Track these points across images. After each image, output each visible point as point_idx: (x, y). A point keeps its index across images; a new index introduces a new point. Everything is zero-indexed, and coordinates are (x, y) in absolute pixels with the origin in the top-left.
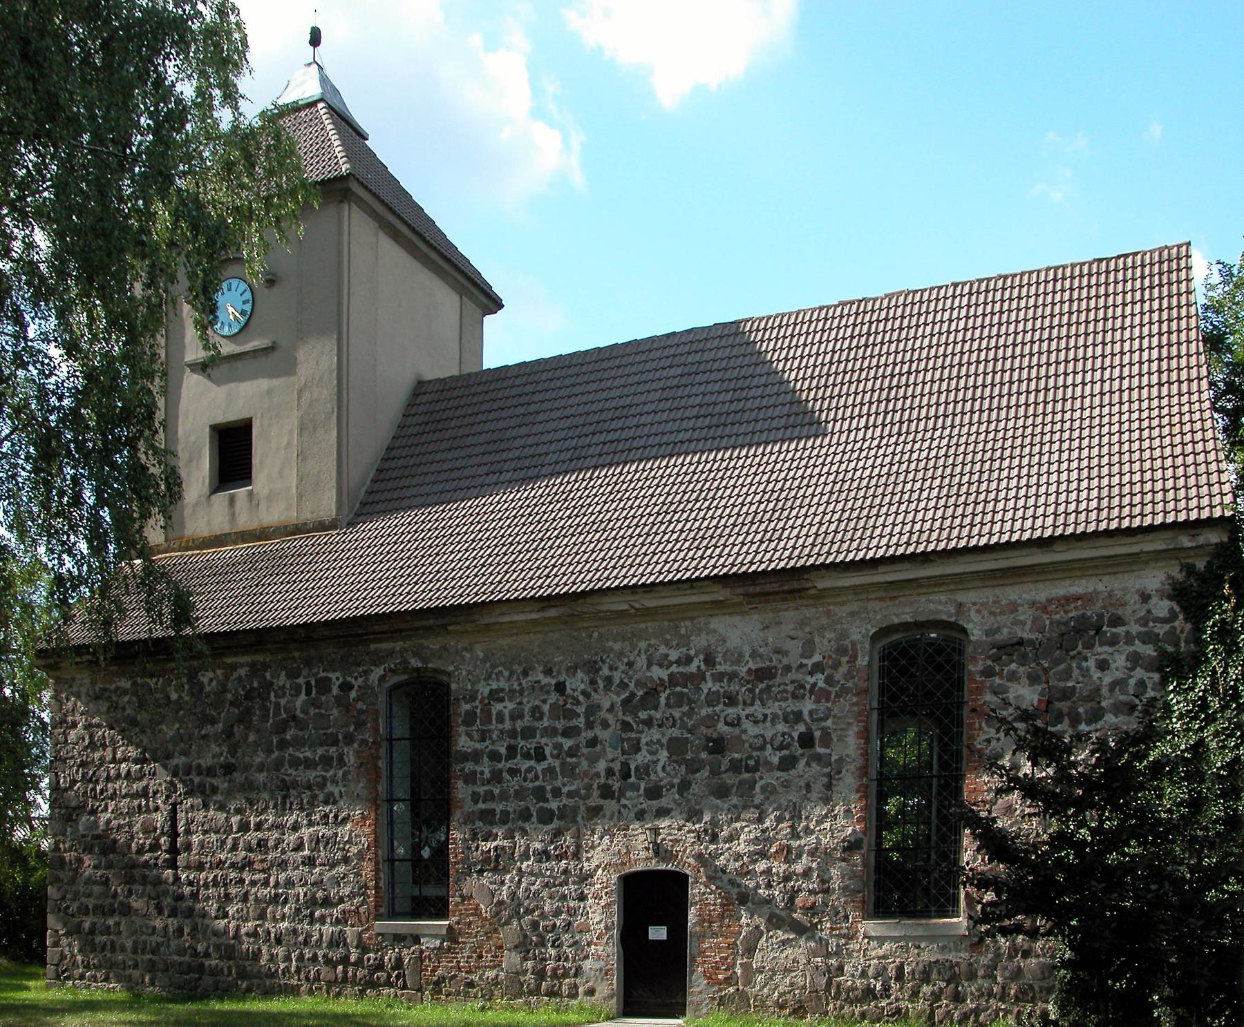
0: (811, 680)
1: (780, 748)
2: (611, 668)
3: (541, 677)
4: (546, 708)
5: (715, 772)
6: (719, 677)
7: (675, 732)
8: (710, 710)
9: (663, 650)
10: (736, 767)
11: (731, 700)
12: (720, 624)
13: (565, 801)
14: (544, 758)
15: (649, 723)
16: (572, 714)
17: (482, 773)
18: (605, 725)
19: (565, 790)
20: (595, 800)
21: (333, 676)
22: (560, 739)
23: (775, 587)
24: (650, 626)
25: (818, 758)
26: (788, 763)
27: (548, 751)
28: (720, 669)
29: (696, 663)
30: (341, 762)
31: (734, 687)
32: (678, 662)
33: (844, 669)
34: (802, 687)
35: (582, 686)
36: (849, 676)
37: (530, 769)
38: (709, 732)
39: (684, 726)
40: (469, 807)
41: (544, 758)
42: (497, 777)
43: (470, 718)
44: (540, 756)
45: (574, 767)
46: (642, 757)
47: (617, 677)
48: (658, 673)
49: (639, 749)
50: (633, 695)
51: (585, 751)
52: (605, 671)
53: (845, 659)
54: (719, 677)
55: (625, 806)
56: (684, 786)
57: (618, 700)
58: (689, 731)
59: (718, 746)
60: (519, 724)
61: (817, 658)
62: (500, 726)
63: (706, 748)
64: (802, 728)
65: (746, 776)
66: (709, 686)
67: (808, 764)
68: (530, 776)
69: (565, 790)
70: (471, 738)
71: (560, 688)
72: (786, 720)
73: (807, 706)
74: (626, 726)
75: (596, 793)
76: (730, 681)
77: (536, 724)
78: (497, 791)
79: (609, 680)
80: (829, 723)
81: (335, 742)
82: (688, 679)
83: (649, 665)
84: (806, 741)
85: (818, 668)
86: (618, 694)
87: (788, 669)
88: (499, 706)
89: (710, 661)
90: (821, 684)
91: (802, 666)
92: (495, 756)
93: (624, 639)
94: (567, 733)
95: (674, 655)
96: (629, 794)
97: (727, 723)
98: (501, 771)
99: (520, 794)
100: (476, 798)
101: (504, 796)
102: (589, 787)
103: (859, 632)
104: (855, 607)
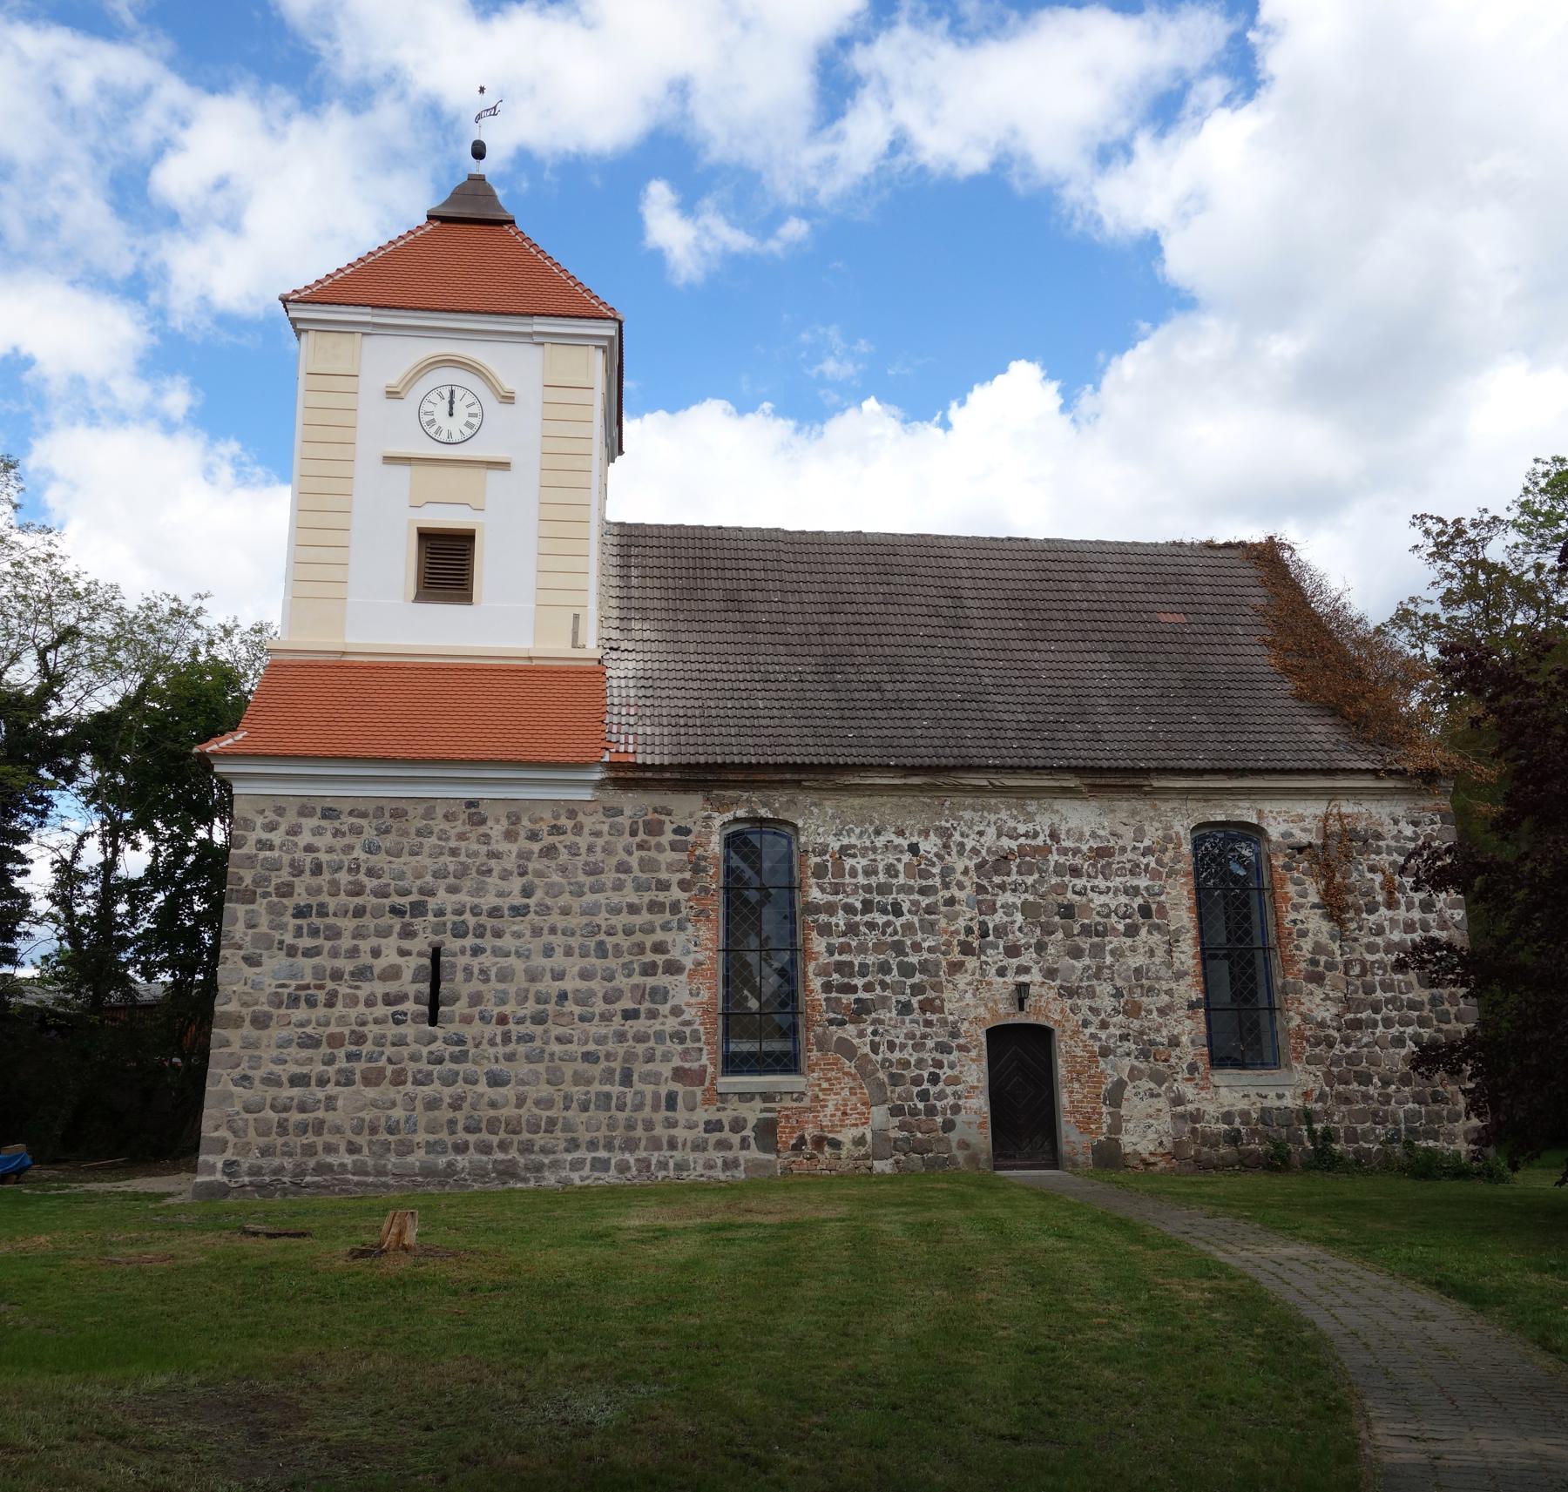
0: (1145, 861)
2: (962, 835)
3: (893, 837)
4: (901, 867)
5: (1068, 934)
6: (1064, 851)
7: (1031, 898)
8: (1059, 879)
9: (1011, 823)
10: (1086, 931)
11: (1075, 872)
13: (926, 955)
14: (902, 914)
15: (1002, 887)
16: (925, 874)
17: (837, 925)
18: (961, 887)
19: (925, 945)
20: (956, 956)
22: (916, 897)
23: (1118, 781)
25: (1158, 928)
26: (1132, 931)
27: (905, 907)
28: (1065, 844)
31: (1078, 861)
32: (1026, 835)
34: (1138, 866)
35: (935, 849)
36: (1176, 860)
37: (888, 924)
38: (1060, 899)
39: (1035, 893)
40: (824, 959)
41: (902, 914)
42: (852, 929)
43: (820, 871)
45: (932, 924)
46: (999, 917)
48: (1006, 843)
49: (995, 911)
50: (984, 862)
51: (943, 909)
52: (957, 837)
53: (1171, 846)
54: (1064, 851)
55: (987, 963)
56: (1041, 947)
57: (971, 864)
58: (1042, 897)
59: (1068, 911)
60: (873, 881)
61: (1147, 843)
62: (854, 881)
63: (1058, 914)
64: (1140, 900)
65: (1096, 939)
66: (1054, 857)
67: (1149, 932)
68: (889, 930)
69: (925, 945)
70: (823, 890)
71: (914, 849)
72: (1126, 892)
73: (1143, 882)
75: (957, 949)
76: (1074, 855)
77: (894, 881)
78: (854, 944)
79: (962, 845)
80: (1163, 898)
82: (1036, 850)
83: (999, 836)
84: (1145, 911)
85: (1147, 852)
86: (971, 859)
87: (1123, 850)
89: (1054, 835)
90: (1153, 865)
91: (1135, 848)
92: (849, 909)
93: (974, 810)
94: (923, 891)
95: (1022, 829)
96: (989, 952)
97: (1075, 892)
98: (857, 924)
99: (879, 947)
100: (830, 950)
101: (862, 949)
102: (948, 944)
103: (1182, 827)
104: (1175, 804)
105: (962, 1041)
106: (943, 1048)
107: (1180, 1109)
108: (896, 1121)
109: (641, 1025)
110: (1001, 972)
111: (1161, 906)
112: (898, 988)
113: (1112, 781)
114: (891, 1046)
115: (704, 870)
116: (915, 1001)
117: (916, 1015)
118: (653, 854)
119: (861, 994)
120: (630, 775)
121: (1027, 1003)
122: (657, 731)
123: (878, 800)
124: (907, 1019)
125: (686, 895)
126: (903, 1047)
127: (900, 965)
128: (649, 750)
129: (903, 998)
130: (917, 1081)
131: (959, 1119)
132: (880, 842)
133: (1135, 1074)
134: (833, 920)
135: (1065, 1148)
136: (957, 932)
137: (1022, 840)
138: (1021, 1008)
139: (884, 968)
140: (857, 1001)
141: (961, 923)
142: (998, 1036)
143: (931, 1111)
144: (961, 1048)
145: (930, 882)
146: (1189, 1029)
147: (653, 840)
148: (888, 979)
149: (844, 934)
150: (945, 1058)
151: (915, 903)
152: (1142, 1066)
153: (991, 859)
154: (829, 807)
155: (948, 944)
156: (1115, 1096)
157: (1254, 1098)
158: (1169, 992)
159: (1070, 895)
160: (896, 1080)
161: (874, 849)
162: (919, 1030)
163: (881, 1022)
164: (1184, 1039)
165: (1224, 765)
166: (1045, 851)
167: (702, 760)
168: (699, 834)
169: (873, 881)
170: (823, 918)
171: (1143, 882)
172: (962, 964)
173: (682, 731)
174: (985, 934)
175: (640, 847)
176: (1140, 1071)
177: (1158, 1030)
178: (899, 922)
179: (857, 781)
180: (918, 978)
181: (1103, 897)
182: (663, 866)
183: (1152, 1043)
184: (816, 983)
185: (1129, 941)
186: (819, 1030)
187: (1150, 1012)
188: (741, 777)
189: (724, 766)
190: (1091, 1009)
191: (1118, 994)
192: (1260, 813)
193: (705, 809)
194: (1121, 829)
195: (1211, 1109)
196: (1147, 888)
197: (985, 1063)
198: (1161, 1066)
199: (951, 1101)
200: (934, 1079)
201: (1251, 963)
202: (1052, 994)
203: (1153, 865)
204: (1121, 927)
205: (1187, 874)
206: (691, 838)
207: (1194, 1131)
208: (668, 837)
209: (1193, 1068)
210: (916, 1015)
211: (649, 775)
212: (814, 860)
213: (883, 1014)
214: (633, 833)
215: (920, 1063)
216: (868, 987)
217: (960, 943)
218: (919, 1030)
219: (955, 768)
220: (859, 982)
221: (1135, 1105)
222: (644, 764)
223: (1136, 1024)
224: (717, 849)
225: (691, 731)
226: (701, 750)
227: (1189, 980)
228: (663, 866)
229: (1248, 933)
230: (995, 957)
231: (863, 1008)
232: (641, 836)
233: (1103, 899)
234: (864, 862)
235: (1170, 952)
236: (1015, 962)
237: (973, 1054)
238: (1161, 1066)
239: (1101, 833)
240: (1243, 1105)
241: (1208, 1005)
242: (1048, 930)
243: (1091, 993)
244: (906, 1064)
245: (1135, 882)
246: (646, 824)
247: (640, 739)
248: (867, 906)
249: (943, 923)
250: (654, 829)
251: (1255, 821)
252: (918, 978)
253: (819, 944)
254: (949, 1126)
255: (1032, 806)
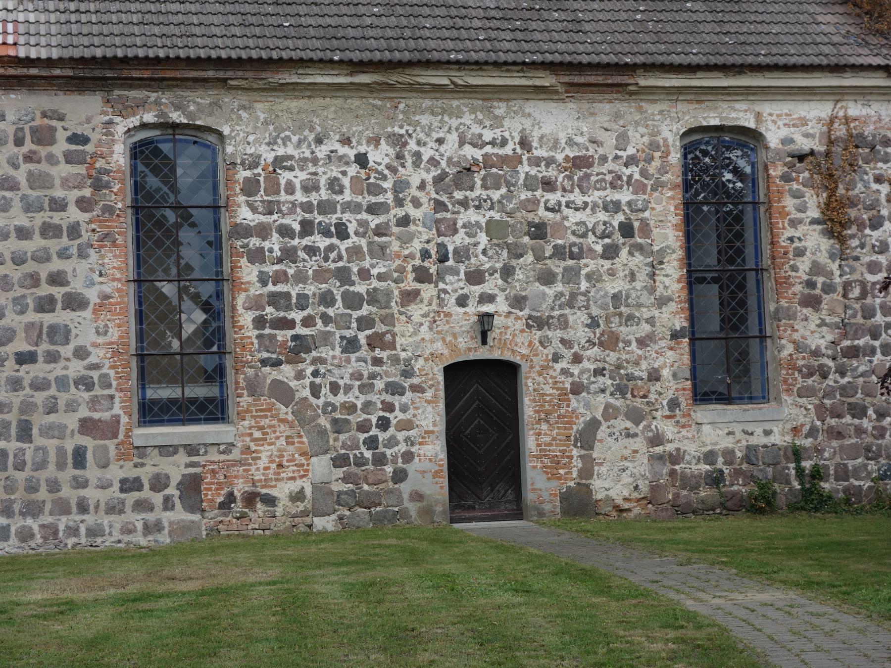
0: (628, 172)
1: (603, 236)
2: (419, 143)
3: (337, 146)
4: (346, 182)
5: (539, 258)
6: (536, 162)
7: (497, 216)
8: (529, 194)
9: (476, 129)
10: (559, 253)
11: (548, 185)
13: (375, 283)
14: (347, 237)
15: (464, 203)
16: (375, 190)
17: (271, 251)
18: (417, 203)
19: (375, 272)
20: (410, 283)
22: (364, 216)
23: (600, 79)
25: (640, 248)
26: (611, 252)
27: (352, 228)
28: (537, 153)
31: (552, 173)
32: (493, 143)
33: (656, 163)
34: (619, 178)
35: (387, 160)
36: (663, 171)
37: (331, 248)
38: (530, 216)
39: (502, 210)
40: (256, 290)
41: (347, 237)
42: (289, 255)
43: (251, 187)
44: (342, 232)
45: (383, 248)
46: (460, 239)
48: (470, 152)
49: (456, 231)
51: (395, 230)
52: (412, 146)
53: (657, 155)
54: (536, 162)
55: (445, 291)
56: (507, 272)
57: (429, 178)
58: (510, 214)
59: (539, 231)
60: (314, 198)
61: (631, 151)
62: (291, 198)
63: (528, 234)
64: (621, 217)
65: (570, 263)
66: (524, 168)
67: (631, 253)
68: (333, 255)
69: (375, 272)
70: (254, 210)
71: (362, 160)
72: (606, 208)
73: (624, 196)
75: (411, 276)
76: (548, 165)
77: (338, 198)
78: (291, 272)
79: (418, 155)
80: (647, 214)
82: (504, 160)
83: (462, 144)
84: (627, 230)
85: (631, 161)
86: (428, 171)
87: (604, 159)
89: (525, 144)
90: (637, 176)
91: (617, 157)
92: (285, 232)
93: (433, 113)
94: (372, 209)
95: (488, 136)
96: (448, 278)
97: (547, 209)
98: (295, 249)
99: (320, 275)
100: (263, 280)
101: (300, 277)
102: (401, 270)
104: (664, 106)
105: (415, 381)
106: (394, 389)
107: (658, 450)
108: (340, 472)
109: (39, 370)
110: (462, 301)
111: (645, 224)
112: (343, 322)
113: (592, 79)
114: (335, 388)
115: (107, 186)
116: (362, 337)
117: (364, 352)
118: (44, 167)
119: (300, 330)
120: (11, 72)
121: (491, 336)
122: (42, 18)
123: (319, 102)
124: (353, 357)
125: (87, 216)
126: (348, 389)
127: (346, 296)
128: (33, 41)
129: (348, 333)
130: (363, 427)
131: (412, 468)
132: (321, 152)
133: (610, 412)
134: (267, 245)
135: (529, 496)
136: (411, 256)
137: (488, 149)
138: (484, 342)
139: (327, 299)
140: (295, 338)
141: (416, 246)
142: (457, 374)
143: (380, 460)
144: (415, 388)
145: (380, 199)
146: (672, 361)
147: (43, 151)
148: (331, 312)
149: (280, 261)
150: (397, 400)
151: (363, 223)
152: (618, 403)
153: (452, 171)
154: (261, 110)
155: (401, 270)
156: (587, 438)
157: (739, 435)
158: (651, 321)
159: (541, 212)
160: (339, 426)
161: (315, 161)
162: (367, 369)
163: (322, 361)
164: (666, 373)
165: (720, 60)
166: (514, 161)
167: (99, 53)
168: (99, 143)
169: (314, 198)
170: (254, 242)
171: (624, 196)
172: (417, 293)
173: (73, 17)
174: (443, 259)
175: (28, 158)
176: (616, 409)
177: (637, 363)
178: (344, 246)
179: (295, 79)
180: (365, 310)
181: (580, 214)
182: (57, 182)
183: (630, 377)
184: (246, 318)
185: (607, 264)
186: (250, 372)
187: (628, 343)
188: (147, 74)
189: (125, 60)
190: (563, 341)
191: (594, 323)
192: (758, 116)
193: (104, 113)
194: (601, 136)
195: (692, 449)
196: (629, 204)
197: (442, 405)
198: (639, 403)
199: (402, 448)
200: (384, 424)
201: (742, 287)
202: (520, 325)
203: (637, 176)
204: (599, 248)
205: (674, 187)
206: (89, 148)
207: (673, 473)
208: (61, 146)
209: (674, 404)
210: (364, 352)
211: (34, 71)
212: (243, 174)
213: (325, 352)
214: (19, 142)
215: (368, 406)
216: (308, 322)
217: (415, 269)
218: (367, 369)
219: (410, 64)
220: (297, 316)
221: (609, 447)
222: (28, 59)
223: (612, 357)
224: (122, 161)
225: (84, 18)
226: (96, 41)
227: (673, 306)
228: (57, 182)
229: (740, 252)
230: (455, 284)
231: (301, 346)
232: (28, 146)
233: (579, 216)
234: (303, 176)
235: (652, 276)
236: (477, 289)
237: (429, 394)
238: (639, 403)
239: (579, 139)
240: (727, 443)
241: (694, 334)
242: (516, 253)
243: (564, 324)
244: (351, 408)
245: (616, 196)
246: (34, 131)
247: (22, 29)
248: (307, 228)
249: (395, 246)
250: (44, 137)
251: (752, 125)
252: (365, 310)
253: (249, 272)
254: (400, 476)
255: (500, 109)
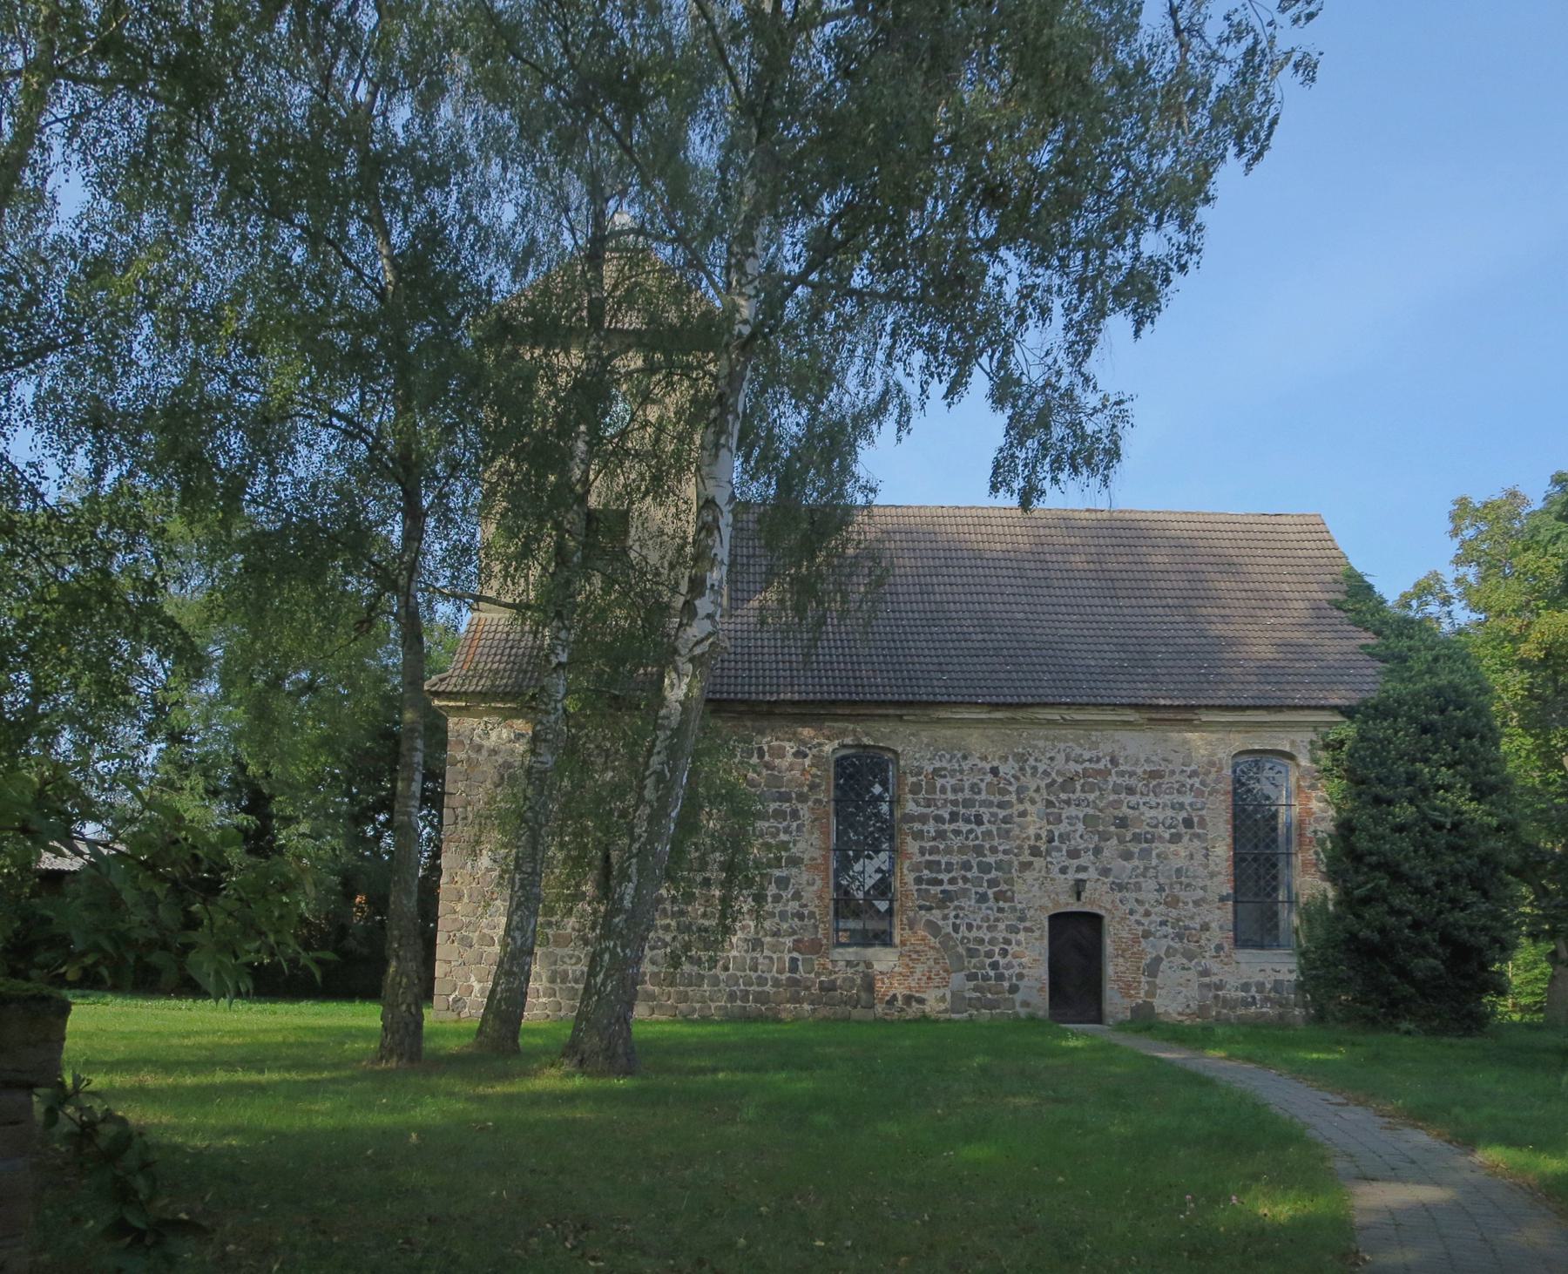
0: (1190, 782)
1: (1170, 827)
3: (978, 761)
4: (983, 786)
5: (1121, 841)
6: (1121, 774)
7: (1091, 811)
8: (1116, 797)
9: (1078, 751)
10: (1136, 838)
11: (1131, 791)
12: (1123, 736)
13: (1001, 856)
15: (1068, 802)
18: (1033, 802)
21: (787, 745)
22: (995, 810)
24: (1069, 733)
25: (1198, 836)
29: (1103, 762)
30: (795, 814)
31: (1133, 782)
32: (1090, 760)
33: (1213, 776)
36: (1217, 781)
37: (971, 831)
38: (1116, 813)
39: (1096, 807)
40: (917, 858)
42: (941, 835)
43: (916, 788)
44: (979, 820)
45: (1008, 831)
47: (1041, 767)
48: (1074, 767)
49: (1061, 821)
50: (1054, 781)
52: (1031, 761)
54: (1121, 774)
56: (1097, 851)
57: (1043, 784)
59: (1122, 823)
60: (960, 797)
61: (1194, 767)
64: (1184, 814)
65: (1145, 845)
66: (1113, 779)
68: (972, 836)
70: (918, 804)
71: (995, 771)
72: (1173, 807)
73: (1187, 799)
74: (1050, 804)
75: (1027, 852)
79: (1035, 768)
80: (1204, 812)
81: (789, 800)
82: (1099, 772)
83: (1067, 759)
84: (1188, 823)
85: (1194, 774)
87: (1173, 773)
88: (942, 781)
89: (1114, 761)
90: (1197, 785)
92: (939, 819)
93: (1047, 739)
94: (1001, 805)
95: (1087, 756)
98: (945, 831)
99: (962, 850)
100: (922, 851)
101: (948, 851)
102: (1020, 847)
103: (1224, 754)
105: (1028, 924)
106: (1013, 929)
107: (1207, 980)
108: (972, 984)
110: (1063, 870)
111: (1202, 819)
112: (977, 882)
113: (1166, 716)
114: (970, 927)
116: (990, 893)
117: (991, 903)
119: (946, 887)
121: (1083, 895)
123: (966, 731)
124: (984, 906)
126: (979, 928)
127: (979, 864)
129: (980, 890)
130: (989, 954)
131: (1022, 984)
132: (966, 766)
133: (1170, 952)
134: (925, 828)
135: (1107, 1008)
136: (1028, 838)
137: (1087, 764)
138: (1079, 899)
139: (967, 866)
140: (943, 892)
141: (1031, 831)
142: (1059, 921)
143: (1000, 977)
144: (1027, 930)
145: (1007, 798)
146: (1220, 918)
148: (969, 875)
149: (934, 839)
150: (1012, 937)
151: (994, 815)
152: (1178, 946)
153: (1060, 780)
154: (925, 737)
155: (1020, 847)
156: (1153, 969)
157: (1269, 972)
158: (1204, 888)
159: (1124, 808)
160: (972, 953)
161: (962, 772)
162: (993, 915)
163: (962, 908)
164: (1214, 925)
165: (1265, 703)
166: (1105, 773)
169: (960, 797)
170: (917, 826)
171: (1187, 799)
172: (1031, 863)
174: (1051, 840)
176: (1176, 950)
177: (1192, 918)
178: (979, 830)
179: (949, 715)
180: (994, 874)
181: (1152, 812)
183: (1187, 928)
184: (910, 878)
186: (911, 914)
187: (1186, 903)
188: (847, 711)
189: (833, 702)
190: (1137, 901)
191: (1161, 889)
192: (1293, 743)
194: (1172, 756)
195: (1232, 982)
196: (1191, 805)
197: (1046, 942)
198: (1192, 946)
199: (1017, 970)
200: (1004, 953)
201: (1274, 866)
202: (1106, 888)
203: (1197, 785)
204: (1167, 836)
205: (1226, 793)
207: (1216, 997)
209: (1219, 948)
210: (991, 903)
212: (911, 780)
213: (964, 903)
215: (992, 941)
216: (952, 881)
217: (1030, 847)
218: (993, 915)
219: (1032, 705)
220: (945, 877)
221: (1169, 974)
223: (1174, 913)
227: (1222, 878)
229: (1274, 841)
230: (1059, 858)
231: (948, 897)
233: (1153, 813)
234: (953, 781)
235: (1206, 856)
236: (1076, 862)
237: (1037, 934)
238: (1192, 946)
239: (1154, 758)
240: (1259, 977)
241: (1238, 897)
242: (1105, 837)
243: (1138, 887)
244: (982, 941)
245: (1181, 799)
248: (954, 817)
249: (1016, 831)
251: (1287, 749)
252: (994, 874)
253: (912, 846)
254: (1014, 989)
255: (1095, 735)
